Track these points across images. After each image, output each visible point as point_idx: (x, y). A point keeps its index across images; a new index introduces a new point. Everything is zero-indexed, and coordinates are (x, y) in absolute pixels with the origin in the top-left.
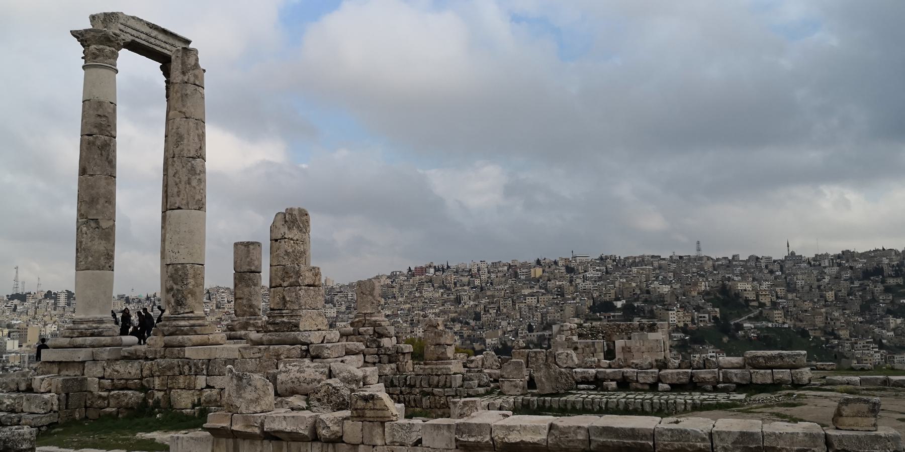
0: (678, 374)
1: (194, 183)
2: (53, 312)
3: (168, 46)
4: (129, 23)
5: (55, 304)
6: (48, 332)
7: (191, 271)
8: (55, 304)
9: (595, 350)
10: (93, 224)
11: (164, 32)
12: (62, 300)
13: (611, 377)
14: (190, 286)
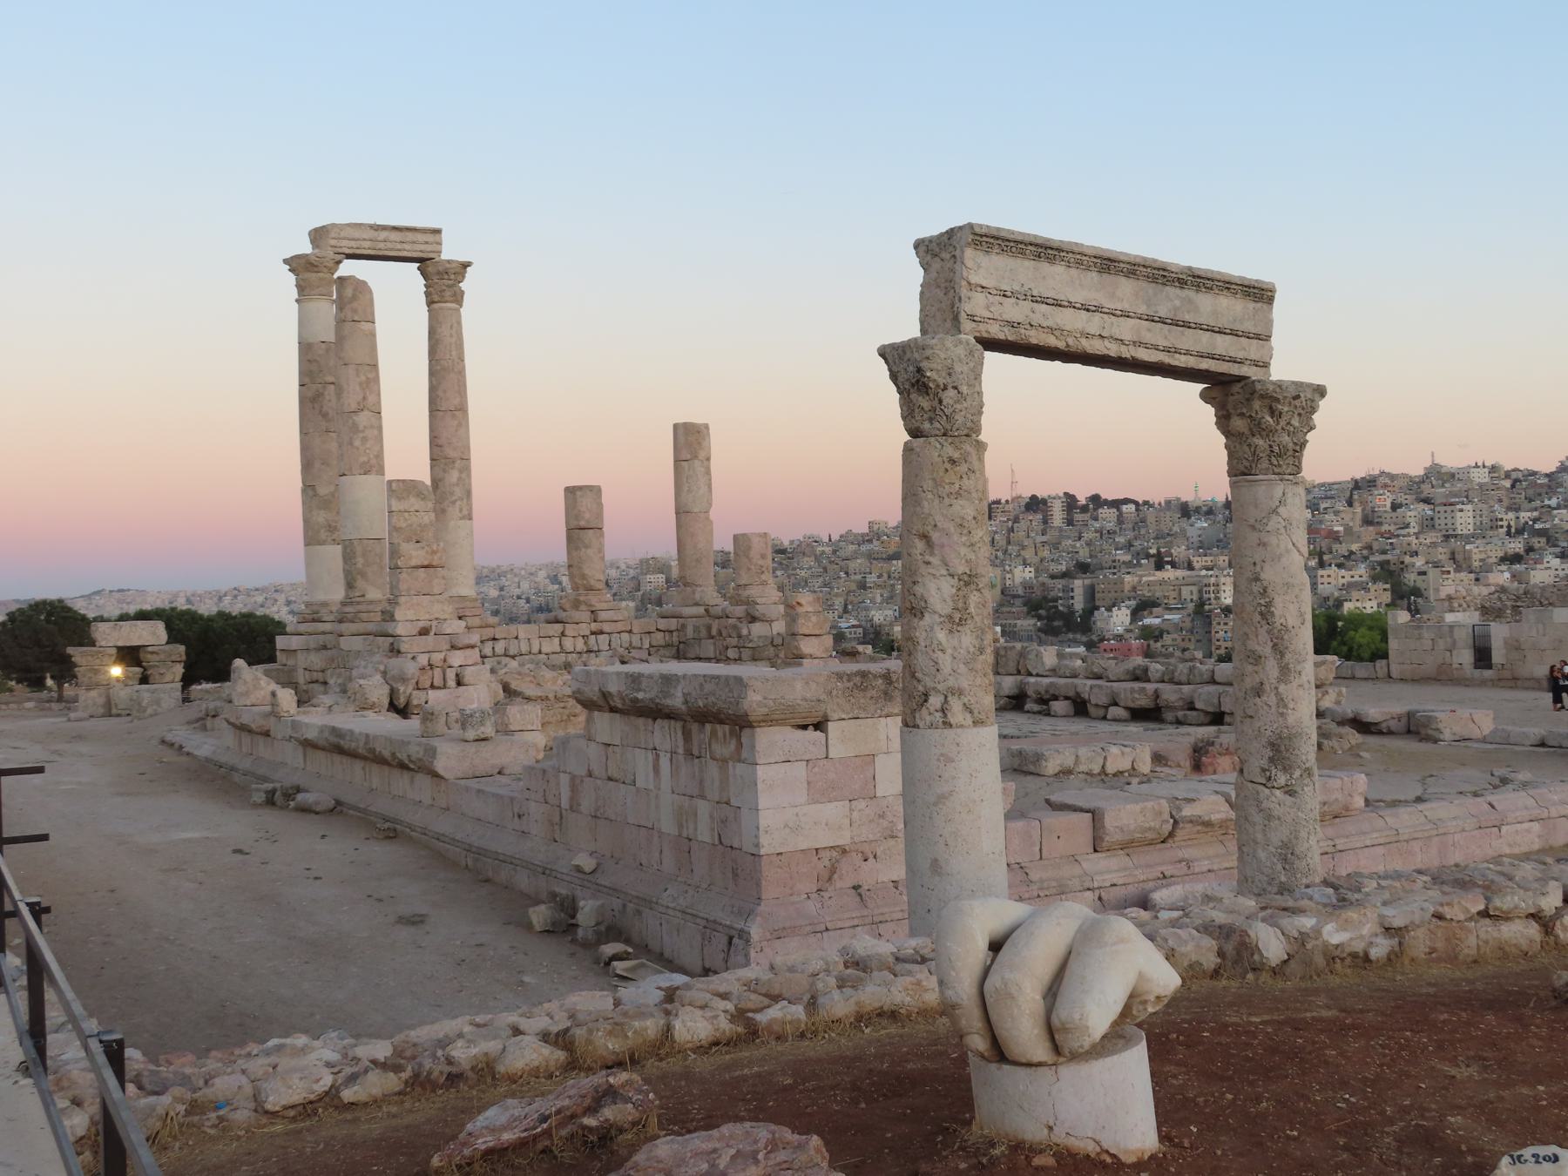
0: (1132, 691)
1: (357, 443)
2: (1040, 539)
3: (407, 247)
4: (343, 234)
5: (1045, 522)
6: (1018, 580)
7: (359, 550)
8: (1045, 522)
9: (1454, 643)
10: (311, 493)
11: (395, 229)
12: (1058, 516)
13: (1063, 692)
14: (359, 566)
